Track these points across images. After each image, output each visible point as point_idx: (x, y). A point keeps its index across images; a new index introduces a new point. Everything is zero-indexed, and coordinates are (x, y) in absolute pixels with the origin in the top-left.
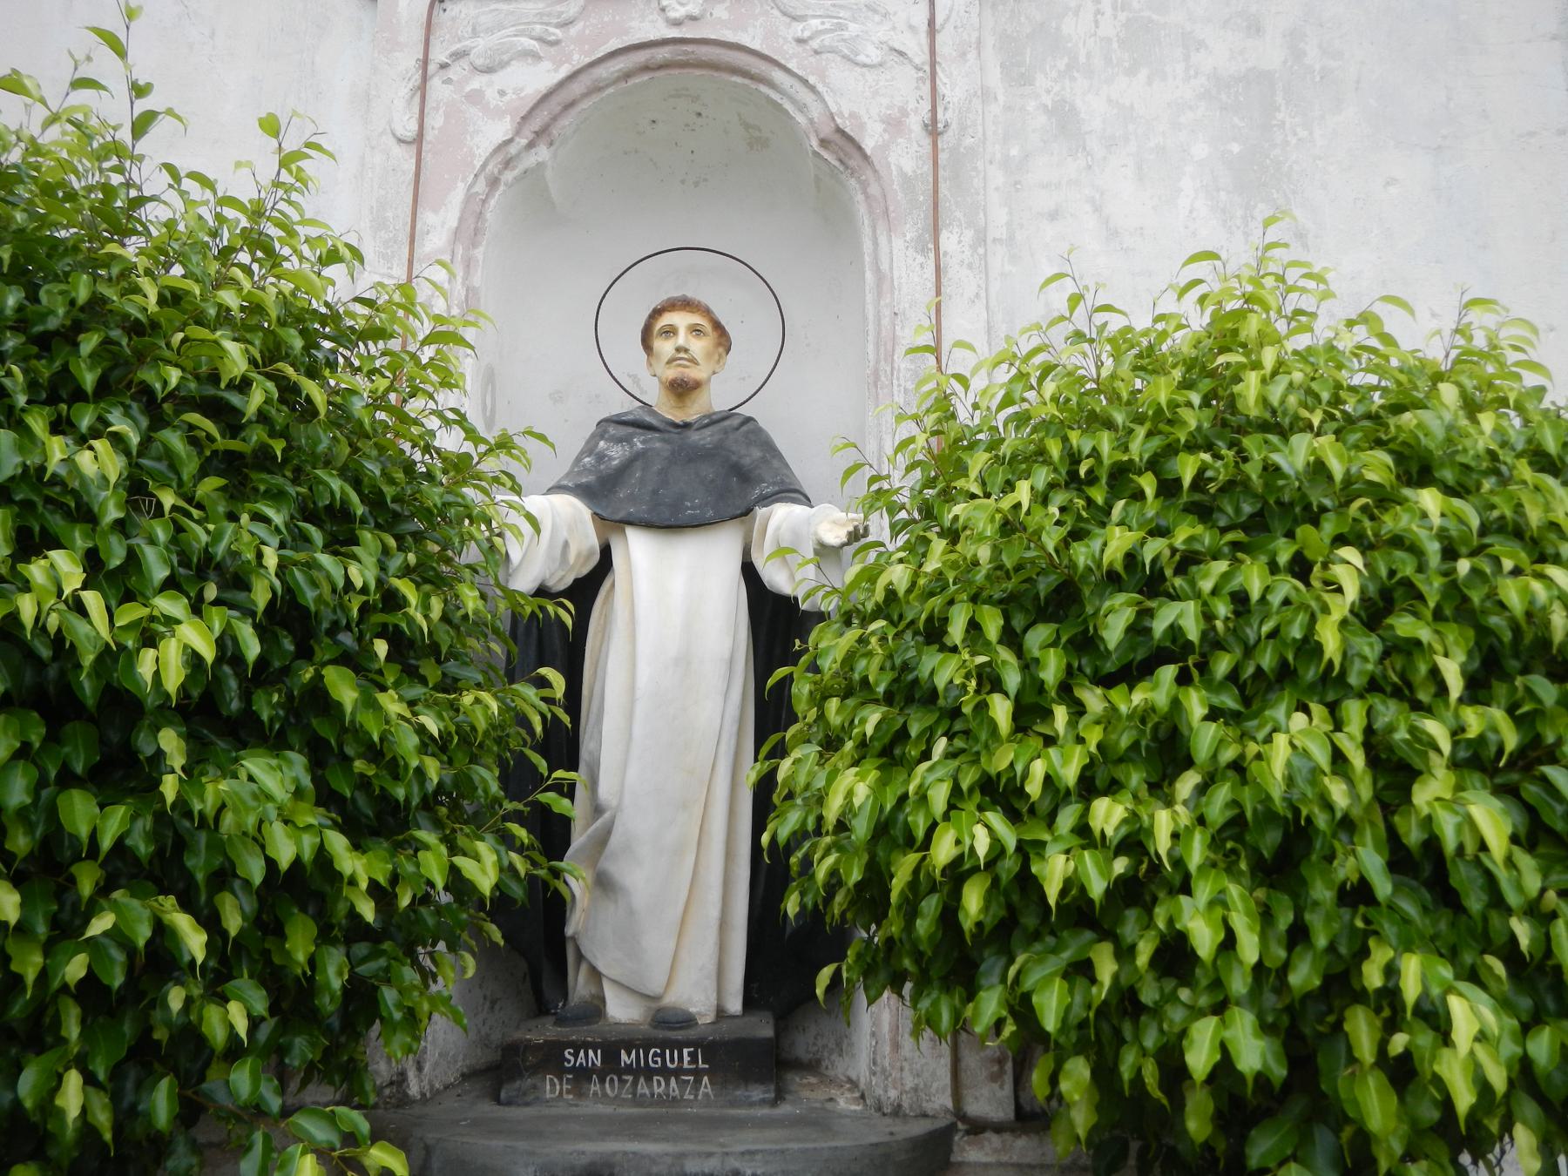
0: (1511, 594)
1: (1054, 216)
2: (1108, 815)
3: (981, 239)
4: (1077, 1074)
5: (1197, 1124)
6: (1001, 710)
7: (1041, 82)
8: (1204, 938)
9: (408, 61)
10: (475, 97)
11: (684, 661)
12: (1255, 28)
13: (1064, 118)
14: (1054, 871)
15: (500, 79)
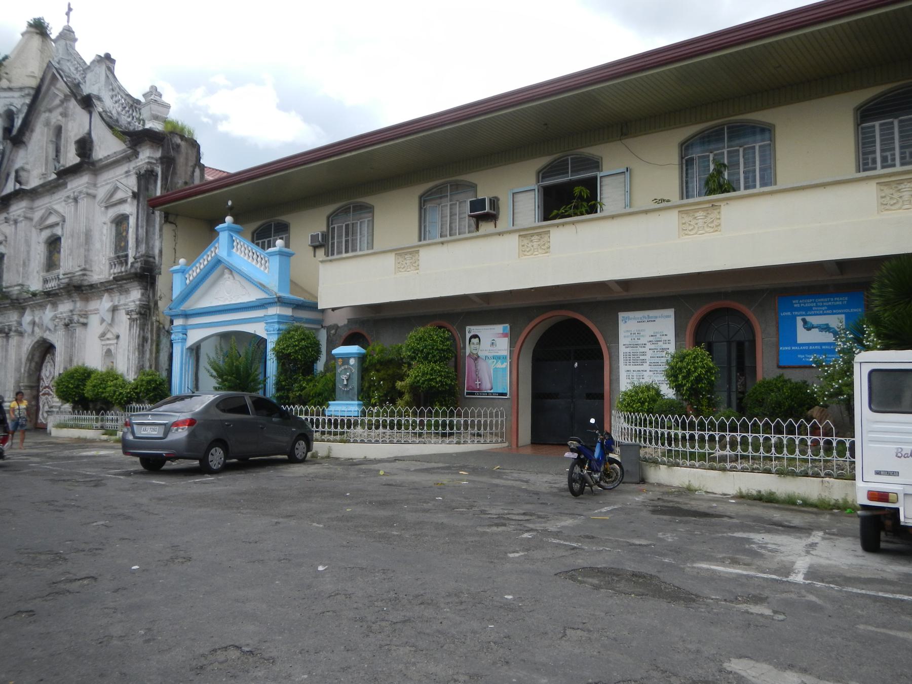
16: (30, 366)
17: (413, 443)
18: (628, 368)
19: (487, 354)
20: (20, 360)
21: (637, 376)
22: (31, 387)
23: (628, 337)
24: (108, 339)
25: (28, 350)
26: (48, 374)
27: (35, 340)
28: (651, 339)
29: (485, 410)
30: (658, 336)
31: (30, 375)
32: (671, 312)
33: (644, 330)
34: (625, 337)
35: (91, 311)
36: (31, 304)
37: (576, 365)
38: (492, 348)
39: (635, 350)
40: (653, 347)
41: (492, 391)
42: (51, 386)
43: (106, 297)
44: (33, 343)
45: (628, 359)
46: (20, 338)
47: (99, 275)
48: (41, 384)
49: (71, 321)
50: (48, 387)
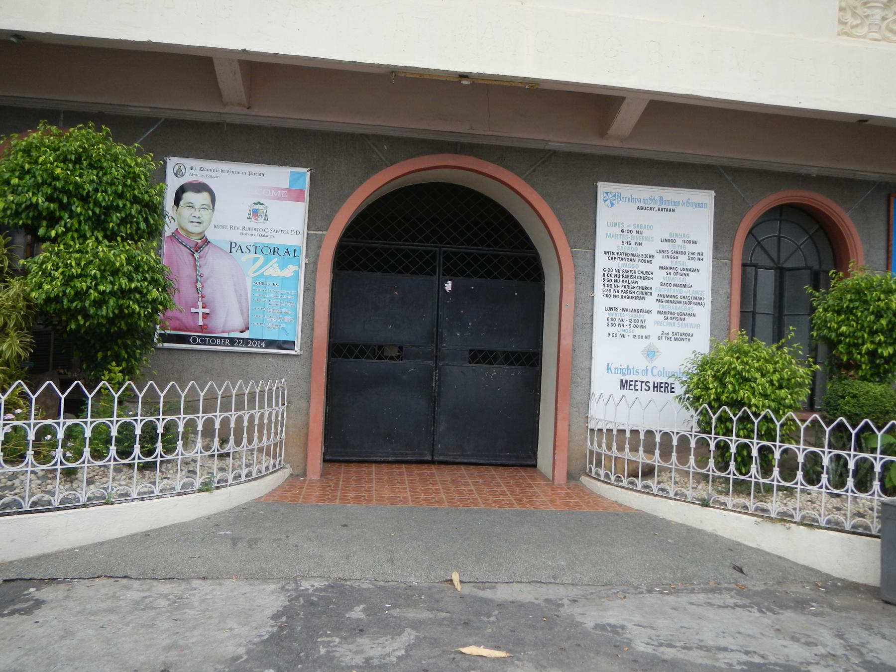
17: (68, 504)
18: (613, 302)
19: (236, 237)
21: (630, 320)
23: (615, 236)
28: (665, 246)
29: (227, 389)
30: (679, 242)
32: (707, 197)
33: (651, 227)
34: (608, 235)
37: (449, 286)
38: (252, 224)
39: (629, 266)
40: (667, 263)
41: (245, 335)
45: (613, 283)
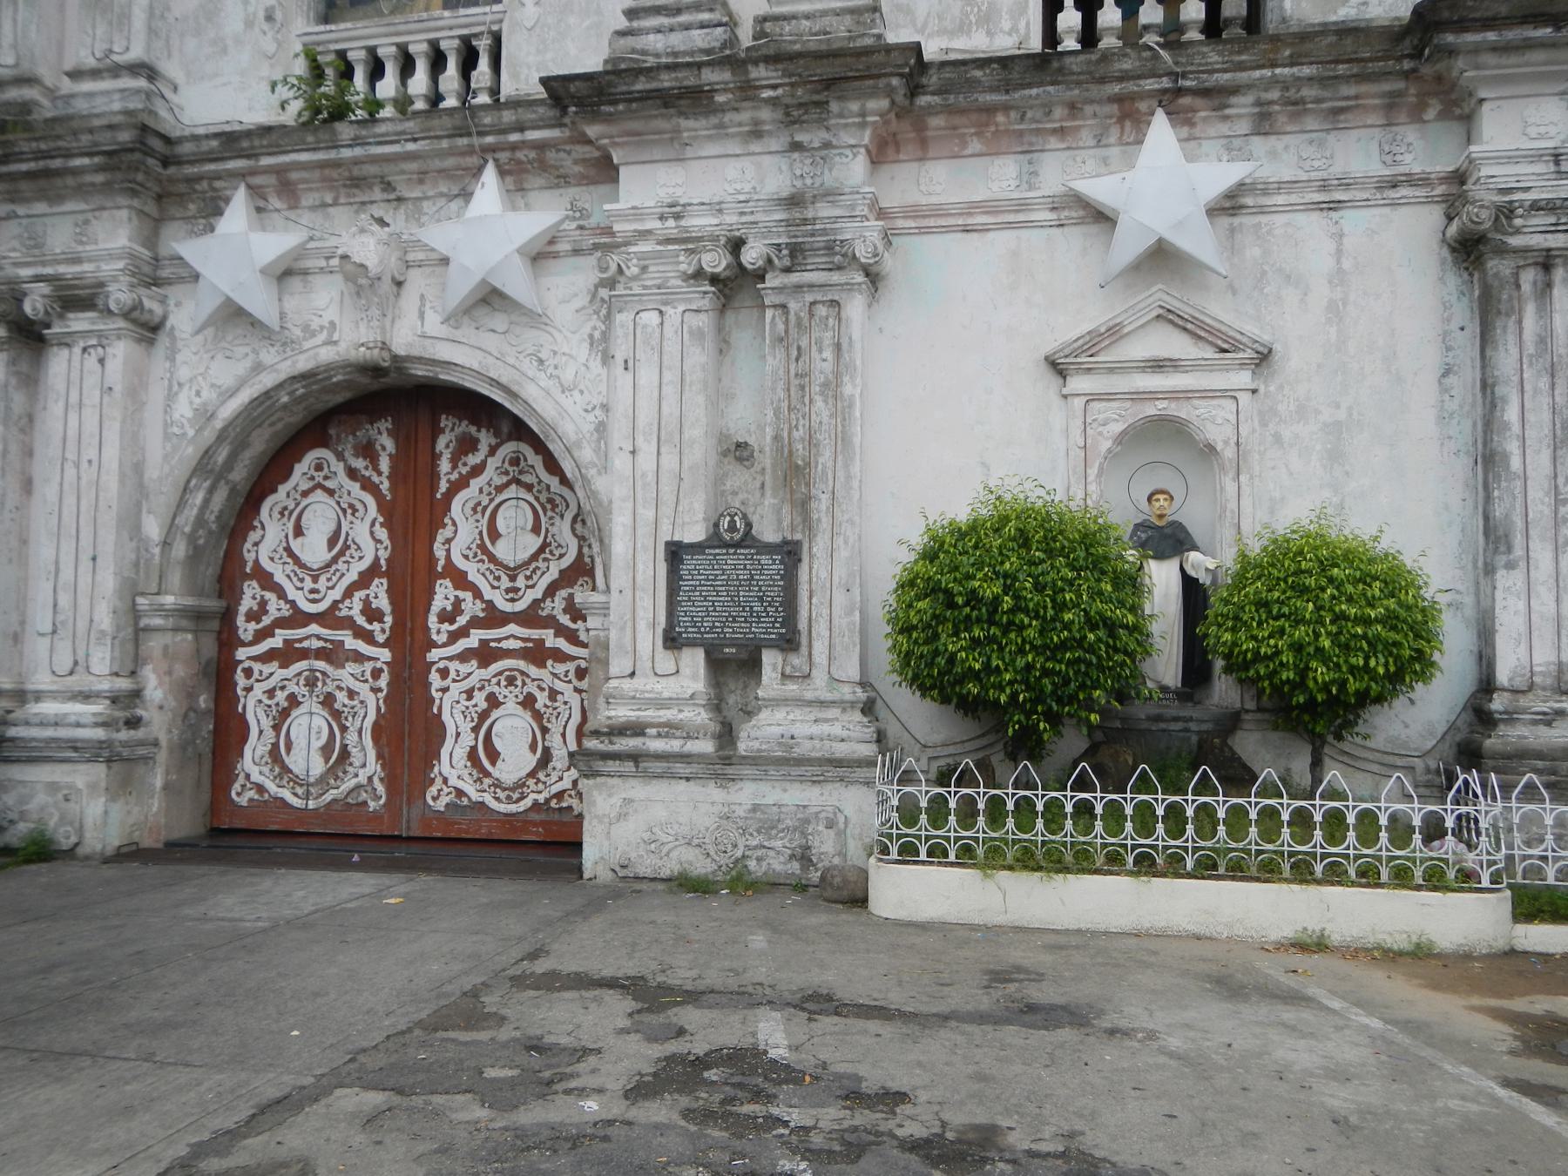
0: (1337, 609)
1: (1273, 468)
2: (1272, 642)
3: (1252, 478)
4: (1266, 683)
5: (1286, 689)
6: (1255, 624)
7: (1271, 426)
8: (1285, 660)
9: (1079, 422)
10: (1100, 434)
11: (1166, 595)
12: (1338, 406)
13: (1278, 439)
14: (1263, 650)
15: (1108, 427)
16: (206, 502)
20: (139, 468)
22: (197, 617)
24: (1158, 365)
25: (205, 415)
26: (314, 549)
27: (303, 364)
31: (196, 556)
35: (914, 212)
36: (280, 171)
42: (354, 608)
43: (1160, 129)
44: (268, 381)
46: (137, 350)
47: (963, 28)
48: (247, 603)
49: (796, 255)
50: (328, 618)
